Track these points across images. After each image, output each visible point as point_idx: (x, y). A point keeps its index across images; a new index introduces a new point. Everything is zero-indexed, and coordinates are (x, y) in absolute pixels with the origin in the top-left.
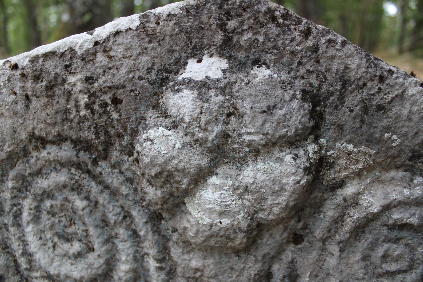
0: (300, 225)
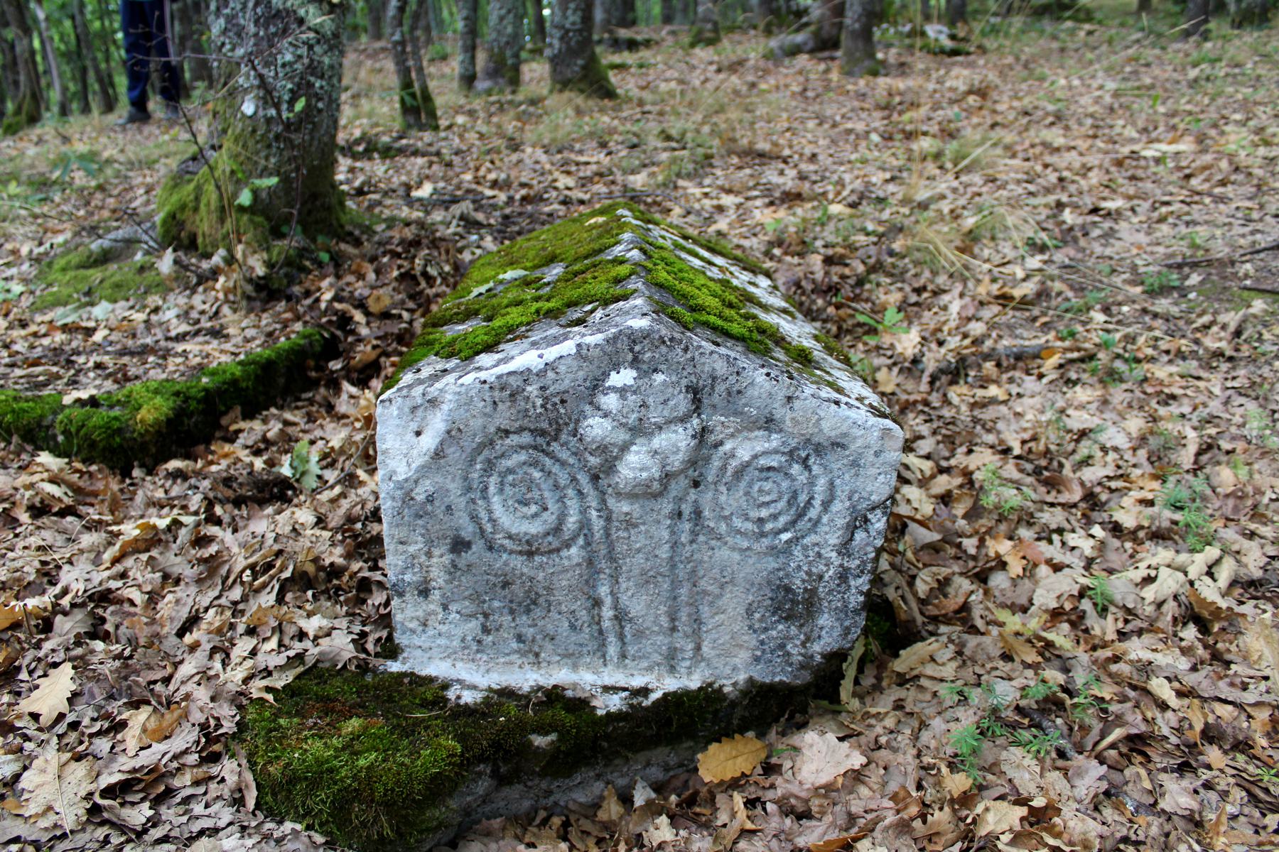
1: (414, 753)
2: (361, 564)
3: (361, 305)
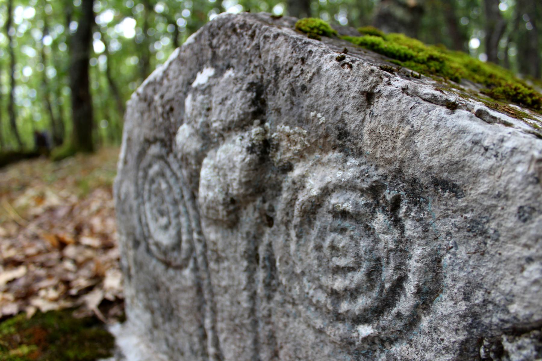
0: (266, 206)
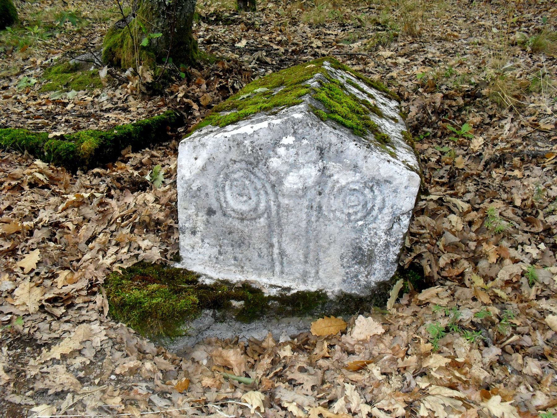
0: (320, 188)
1: (178, 300)
2: (171, 220)
3: (197, 101)
